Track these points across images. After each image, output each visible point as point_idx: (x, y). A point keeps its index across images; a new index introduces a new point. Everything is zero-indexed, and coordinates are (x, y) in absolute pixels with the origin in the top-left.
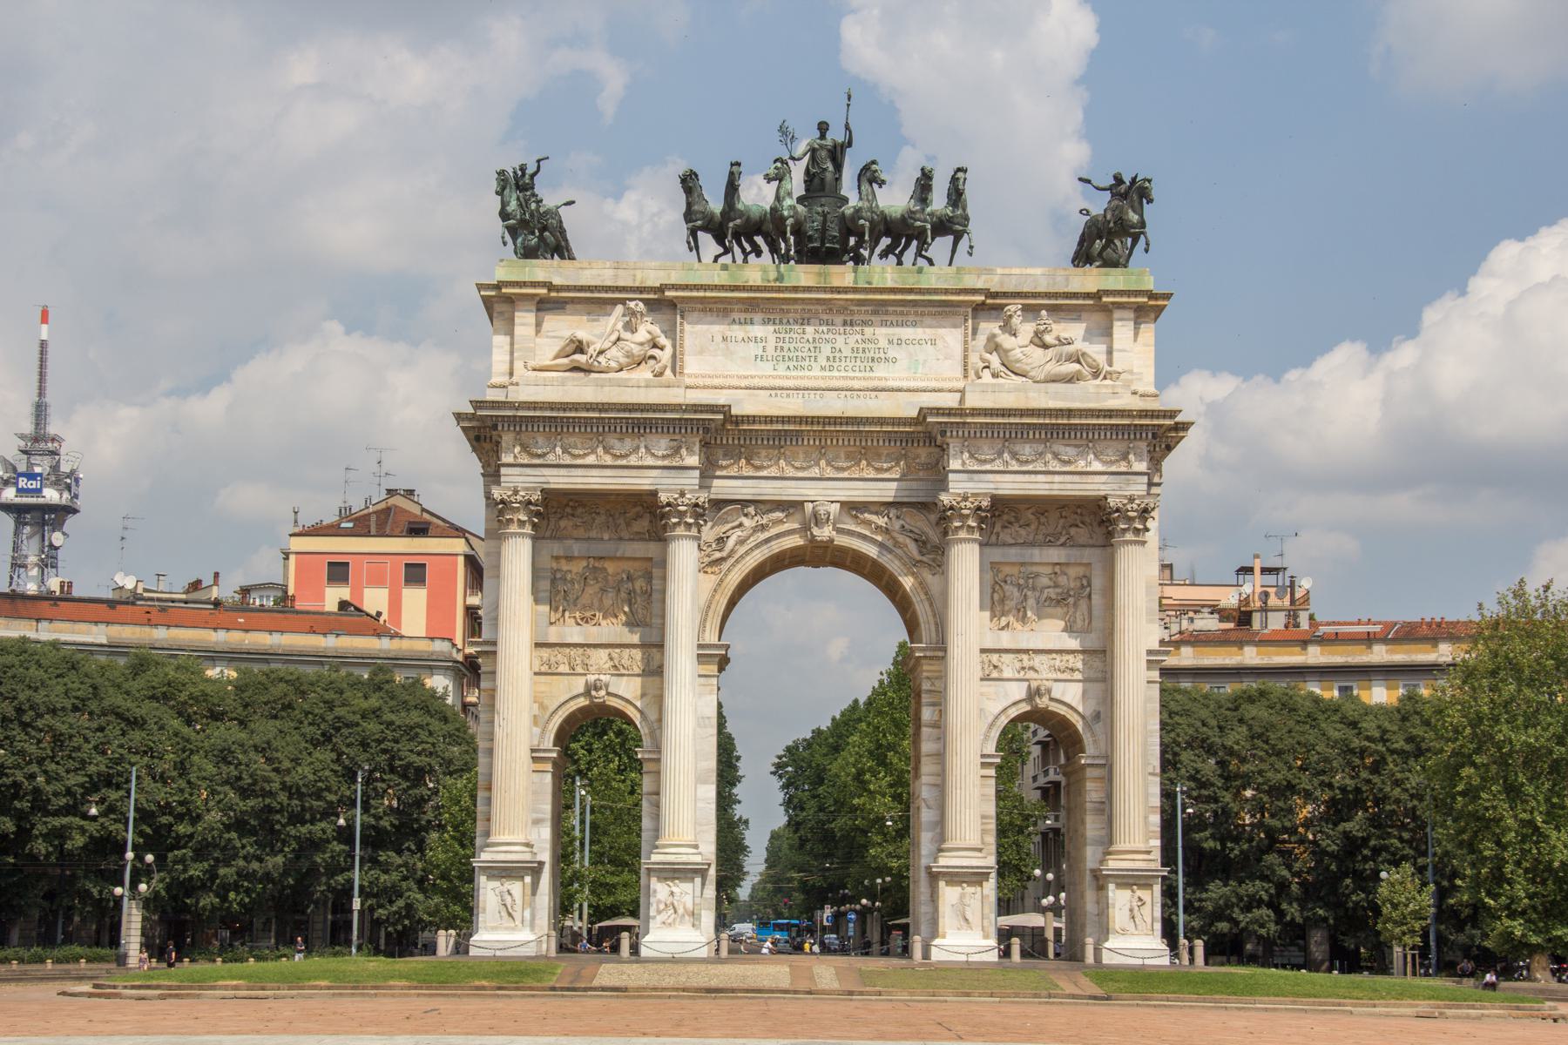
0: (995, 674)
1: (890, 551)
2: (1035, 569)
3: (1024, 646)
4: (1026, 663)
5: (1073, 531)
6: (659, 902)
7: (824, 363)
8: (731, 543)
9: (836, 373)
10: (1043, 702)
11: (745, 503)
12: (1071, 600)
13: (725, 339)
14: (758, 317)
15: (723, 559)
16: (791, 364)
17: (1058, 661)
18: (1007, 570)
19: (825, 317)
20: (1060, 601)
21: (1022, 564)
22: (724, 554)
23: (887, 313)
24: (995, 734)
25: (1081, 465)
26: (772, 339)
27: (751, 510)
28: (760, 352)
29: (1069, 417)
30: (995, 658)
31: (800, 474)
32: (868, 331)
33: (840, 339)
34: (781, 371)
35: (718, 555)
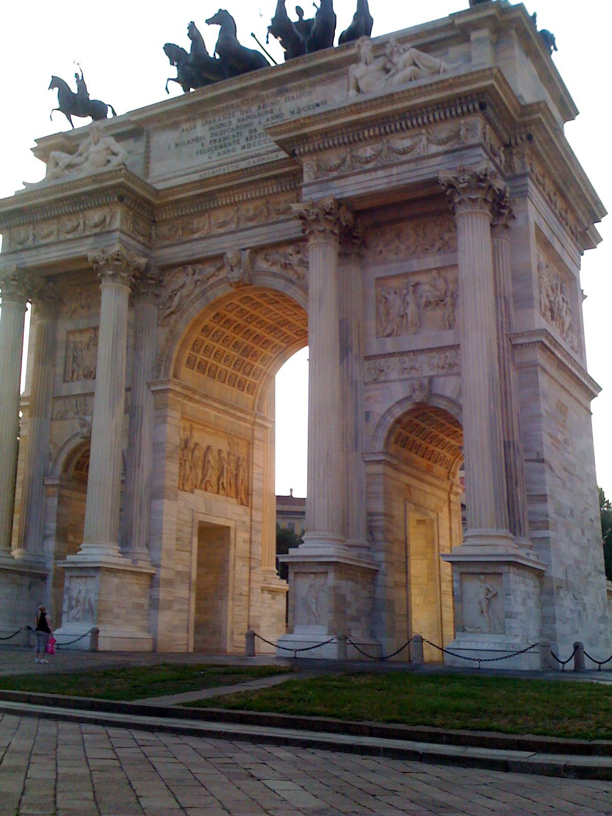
0: (382, 379)
1: (292, 282)
2: (416, 279)
3: (406, 349)
4: (407, 365)
5: (447, 236)
6: (70, 599)
7: (243, 142)
8: (176, 299)
9: (253, 148)
10: (418, 397)
11: (184, 265)
12: (448, 300)
13: (177, 145)
14: (199, 123)
15: (172, 313)
16: (221, 151)
17: (437, 359)
18: (394, 283)
19: (244, 108)
20: (440, 302)
21: (406, 275)
22: (172, 309)
23: (287, 91)
24: (383, 434)
25: (418, 152)
26: (208, 136)
27: (190, 269)
28: (200, 148)
29: (392, 102)
30: (382, 361)
31: (221, 231)
32: (276, 109)
33: (255, 121)
34: (214, 157)
35: (168, 311)
